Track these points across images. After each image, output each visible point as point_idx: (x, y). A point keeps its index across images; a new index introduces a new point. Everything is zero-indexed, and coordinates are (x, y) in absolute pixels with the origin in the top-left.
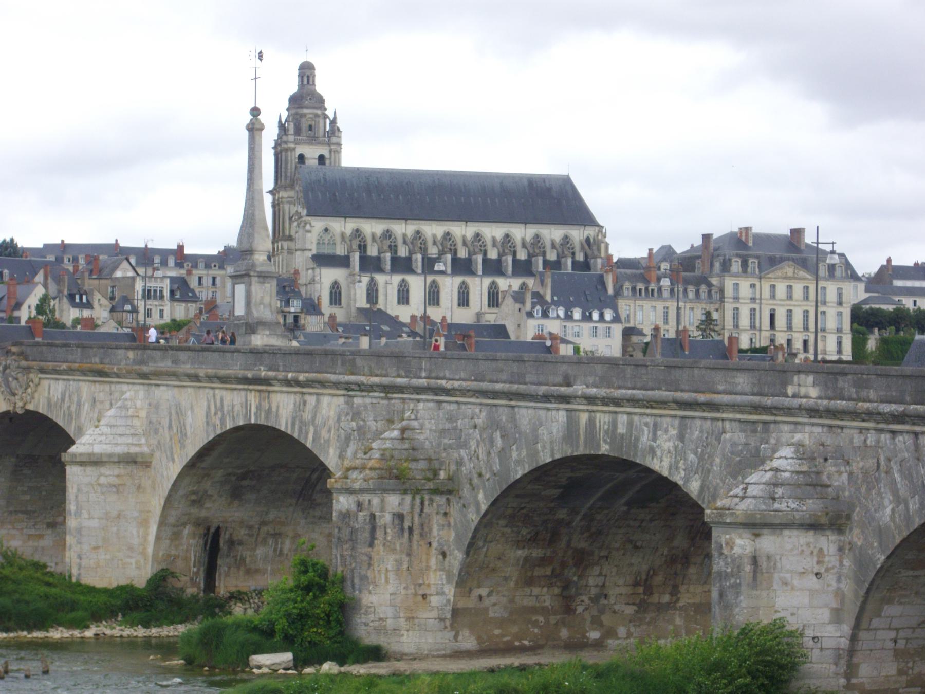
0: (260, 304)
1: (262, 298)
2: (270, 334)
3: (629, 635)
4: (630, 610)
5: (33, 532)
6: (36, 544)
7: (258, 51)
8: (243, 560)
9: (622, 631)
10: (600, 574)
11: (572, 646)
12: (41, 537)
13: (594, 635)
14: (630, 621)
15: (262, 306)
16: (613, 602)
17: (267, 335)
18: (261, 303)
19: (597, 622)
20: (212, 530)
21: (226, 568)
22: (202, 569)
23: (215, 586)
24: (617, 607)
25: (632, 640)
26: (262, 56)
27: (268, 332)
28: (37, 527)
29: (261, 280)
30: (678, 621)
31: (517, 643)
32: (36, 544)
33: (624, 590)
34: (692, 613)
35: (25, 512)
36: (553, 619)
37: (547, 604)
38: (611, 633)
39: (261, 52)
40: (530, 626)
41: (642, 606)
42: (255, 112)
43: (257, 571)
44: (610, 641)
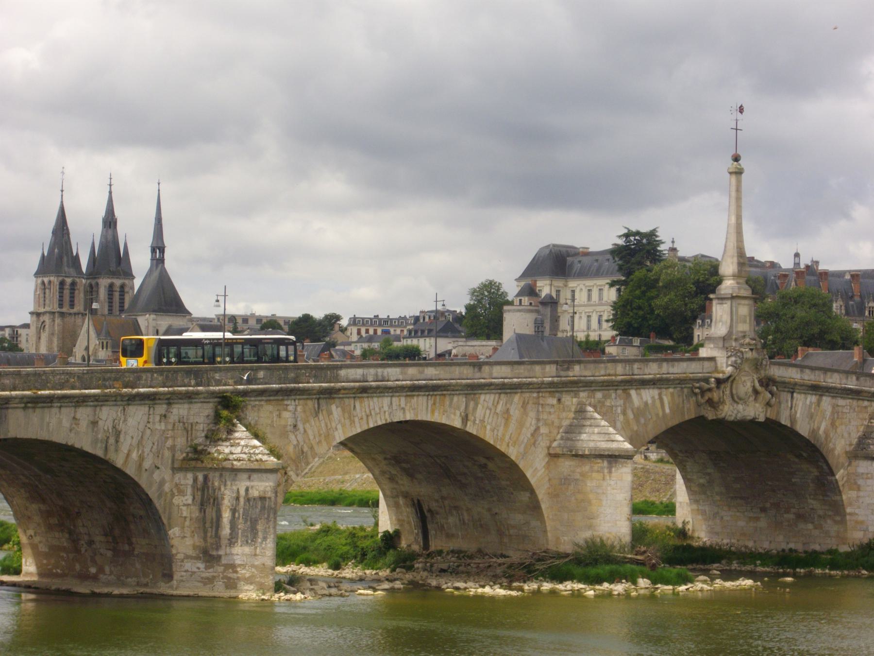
0: (720, 321)
1: (721, 316)
2: (714, 347)
3: (111, 573)
4: (109, 554)
5: (751, 515)
6: (755, 525)
7: (739, 106)
8: (443, 527)
9: (107, 569)
10: (83, 526)
11: (84, 577)
12: (757, 519)
13: (93, 570)
14: (111, 562)
15: (721, 323)
16: (99, 547)
17: (711, 348)
18: (720, 321)
19: (94, 561)
20: (416, 502)
21: (434, 532)
22: (420, 531)
23: (429, 546)
24: (102, 551)
25: (113, 576)
26: (743, 109)
27: (712, 346)
28: (753, 510)
29: (720, 302)
30: (138, 566)
31: (54, 571)
32: (755, 525)
33: (102, 539)
34: (144, 560)
35: (742, 498)
36: (71, 556)
37: (65, 544)
38: (101, 570)
39: (741, 106)
40: (60, 560)
41: (116, 551)
42: (736, 159)
43: (453, 535)
44: (101, 576)
